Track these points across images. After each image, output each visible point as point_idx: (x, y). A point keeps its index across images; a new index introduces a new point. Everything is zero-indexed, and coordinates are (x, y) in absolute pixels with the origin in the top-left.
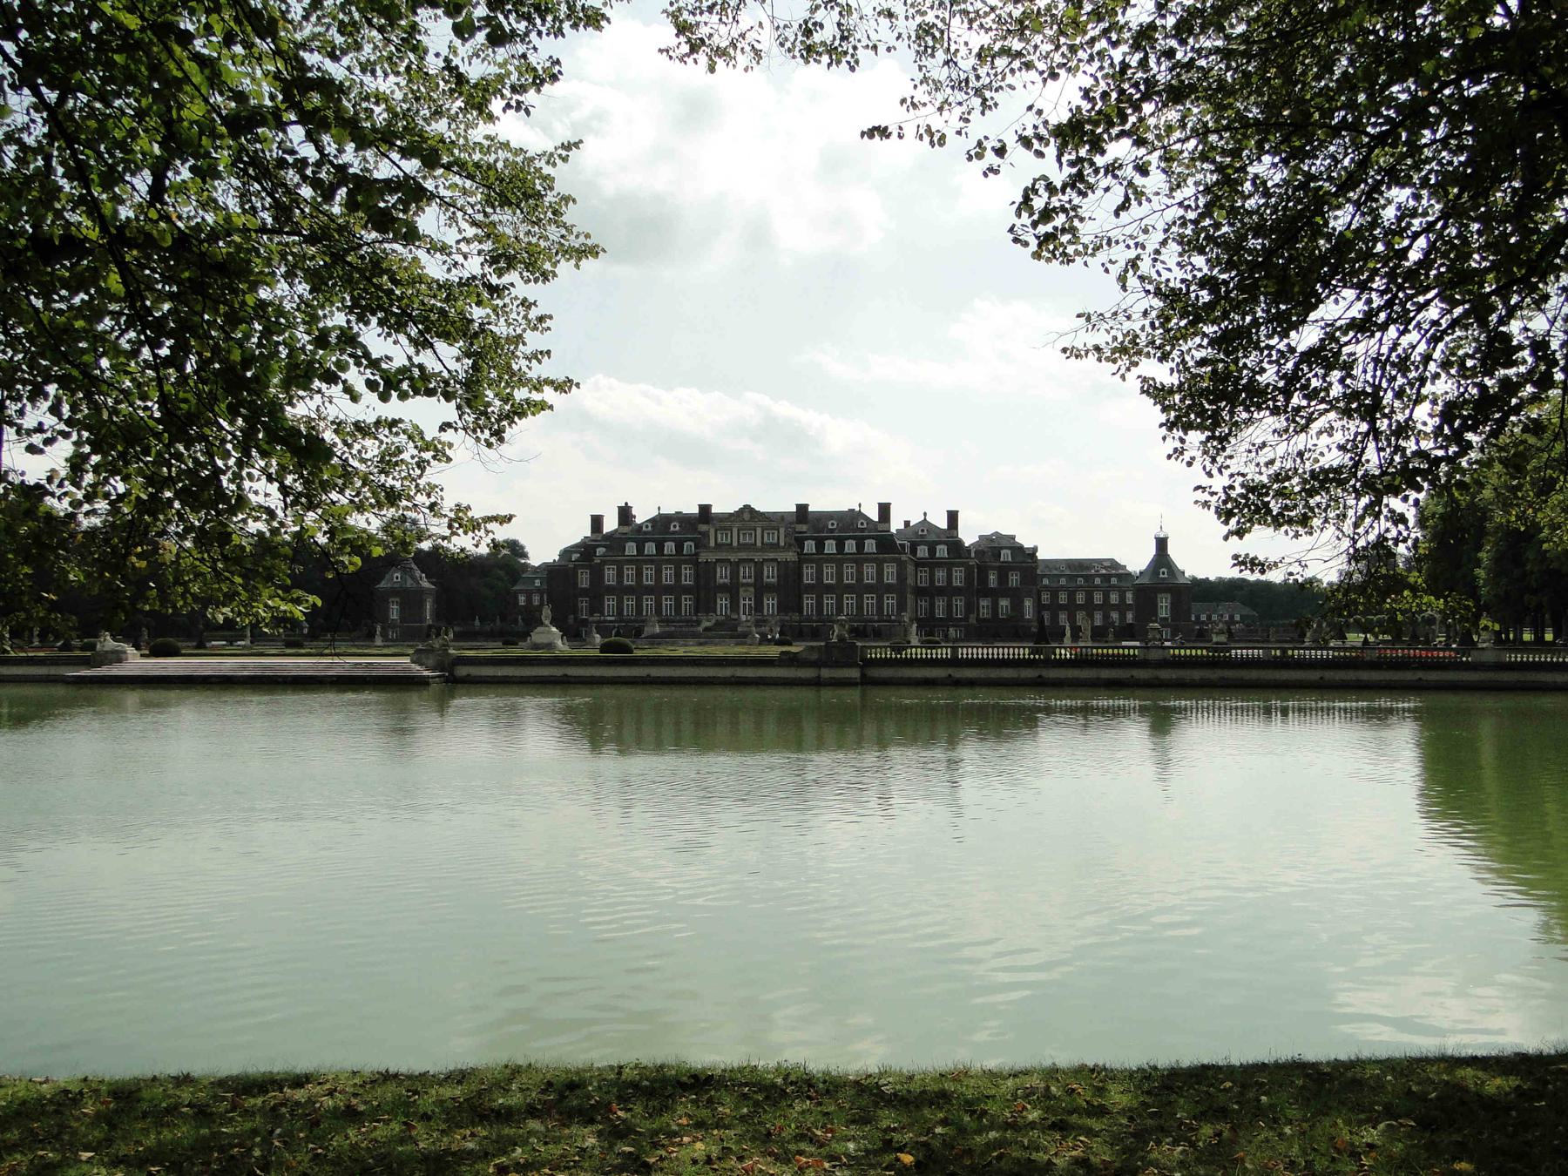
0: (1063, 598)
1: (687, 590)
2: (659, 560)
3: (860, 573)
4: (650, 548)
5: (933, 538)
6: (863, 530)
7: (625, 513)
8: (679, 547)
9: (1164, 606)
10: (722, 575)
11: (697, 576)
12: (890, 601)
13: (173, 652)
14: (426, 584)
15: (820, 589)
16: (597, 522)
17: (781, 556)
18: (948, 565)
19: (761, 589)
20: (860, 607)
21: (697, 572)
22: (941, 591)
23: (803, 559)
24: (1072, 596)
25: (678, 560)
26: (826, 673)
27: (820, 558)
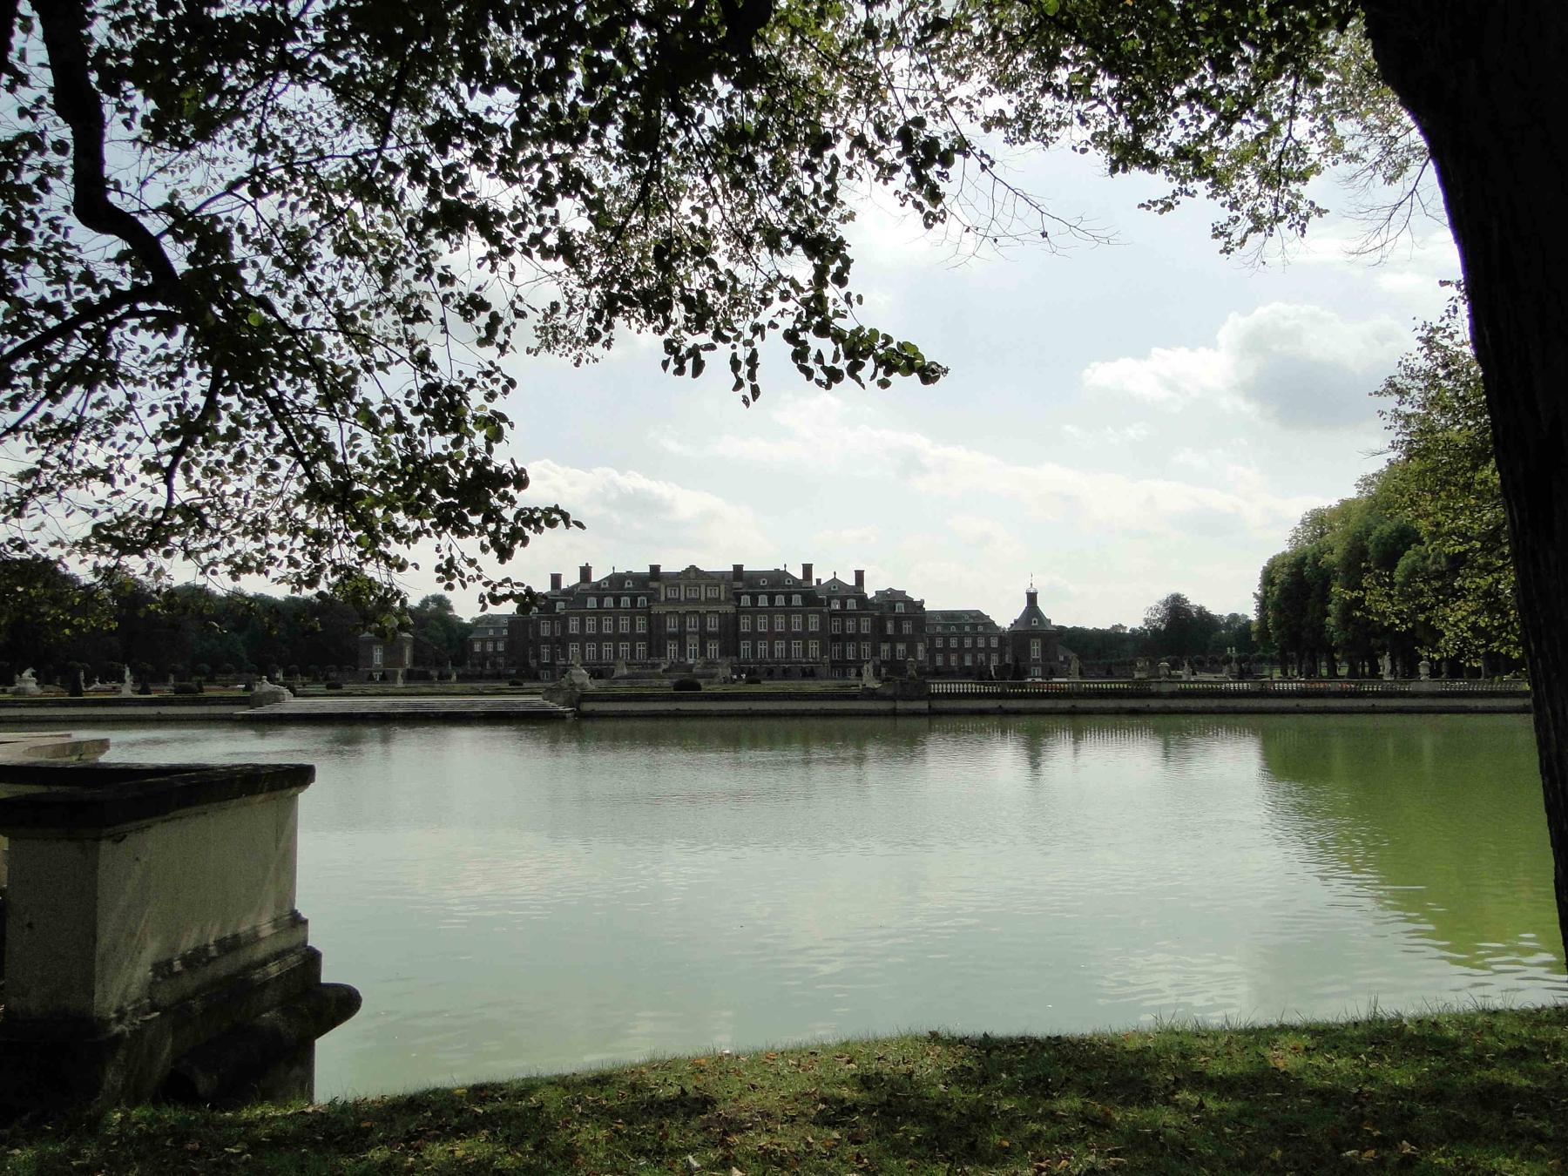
0: (954, 643)
1: (641, 637)
2: (615, 612)
3: (788, 623)
7: (585, 572)
8: (634, 602)
9: (1036, 649)
10: (672, 625)
16: (556, 579)
17: (722, 609)
19: (704, 637)
20: (788, 650)
21: (649, 624)
22: (852, 638)
24: (946, 641)
25: (633, 612)
26: (900, 705)
27: (755, 610)
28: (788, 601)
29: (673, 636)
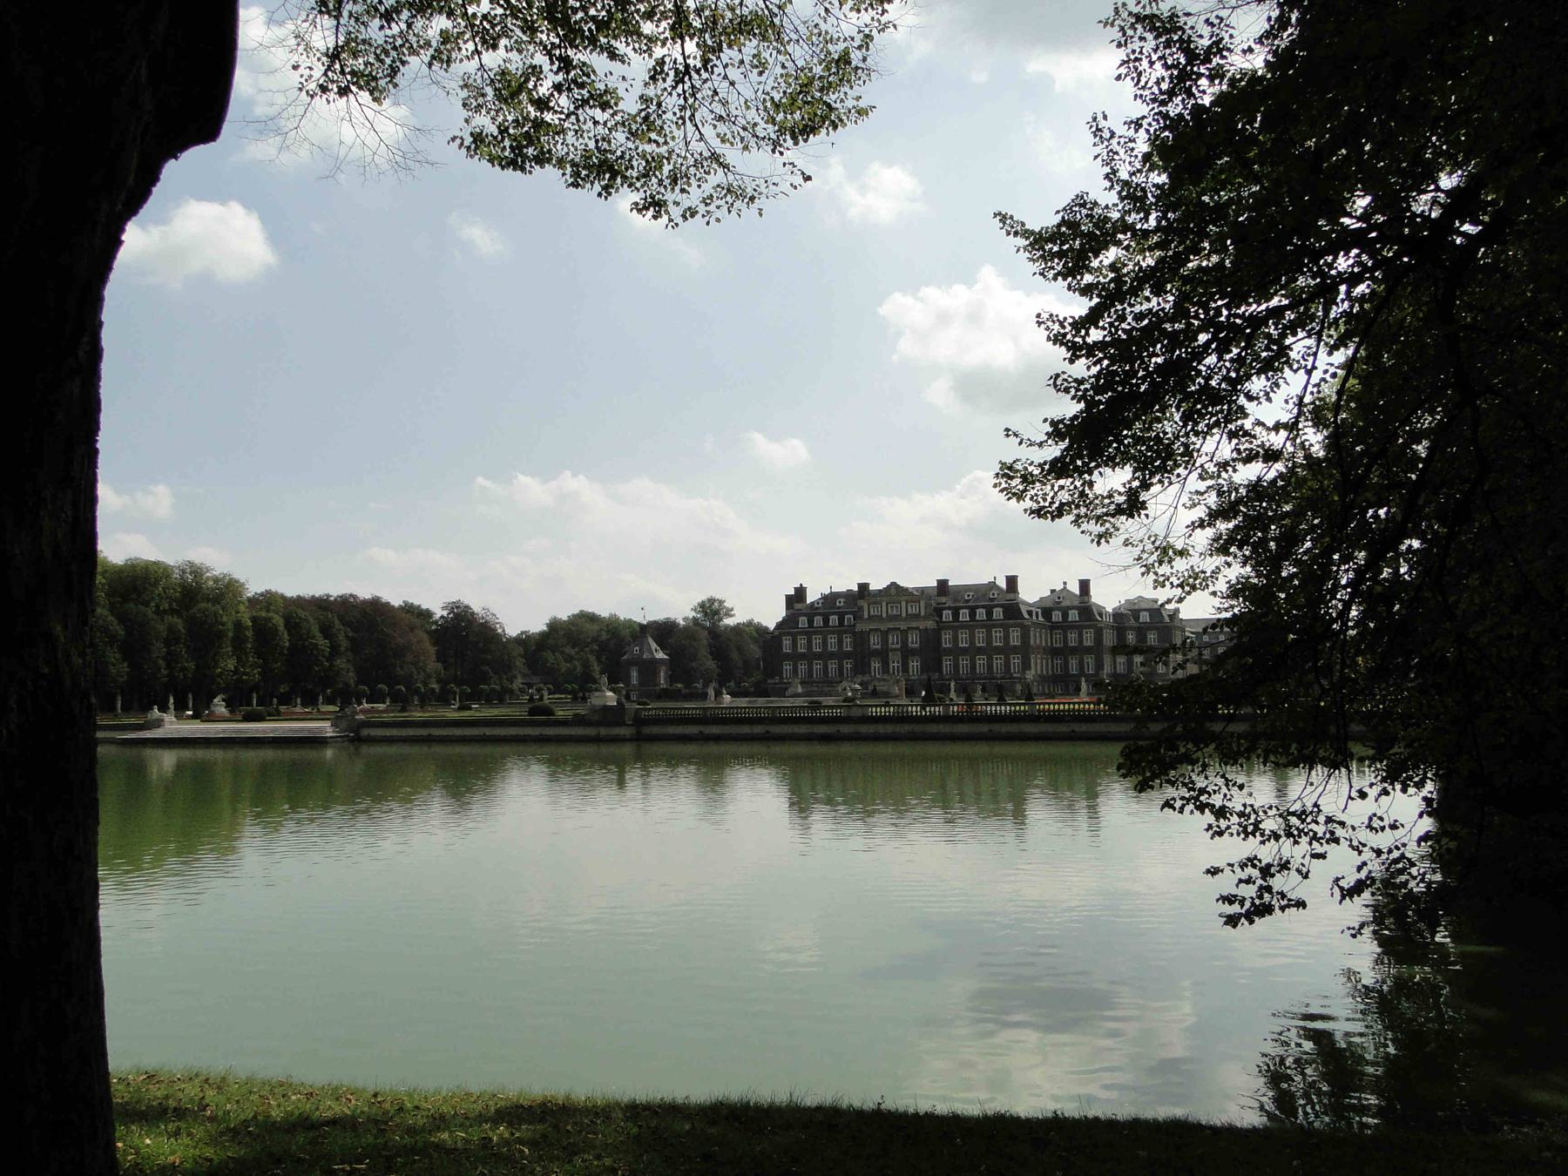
1: (848, 655)
3: (989, 637)
4: (818, 621)
5: (1066, 603)
6: (992, 600)
8: (841, 620)
10: (875, 642)
11: (855, 644)
12: (1016, 661)
13: (276, 715)
14: (660, 655)
15: (956, 652)
17: (922, 625)
18: (1078, 627)
19: (907, 653)
22: (1074, 651)
23: (941, 626)
25: (840, 630)
26: (603, 731)
27: (956, 624)
28: (973, 614)
29: (876, 653)
